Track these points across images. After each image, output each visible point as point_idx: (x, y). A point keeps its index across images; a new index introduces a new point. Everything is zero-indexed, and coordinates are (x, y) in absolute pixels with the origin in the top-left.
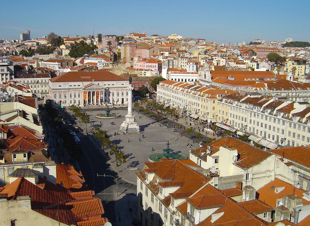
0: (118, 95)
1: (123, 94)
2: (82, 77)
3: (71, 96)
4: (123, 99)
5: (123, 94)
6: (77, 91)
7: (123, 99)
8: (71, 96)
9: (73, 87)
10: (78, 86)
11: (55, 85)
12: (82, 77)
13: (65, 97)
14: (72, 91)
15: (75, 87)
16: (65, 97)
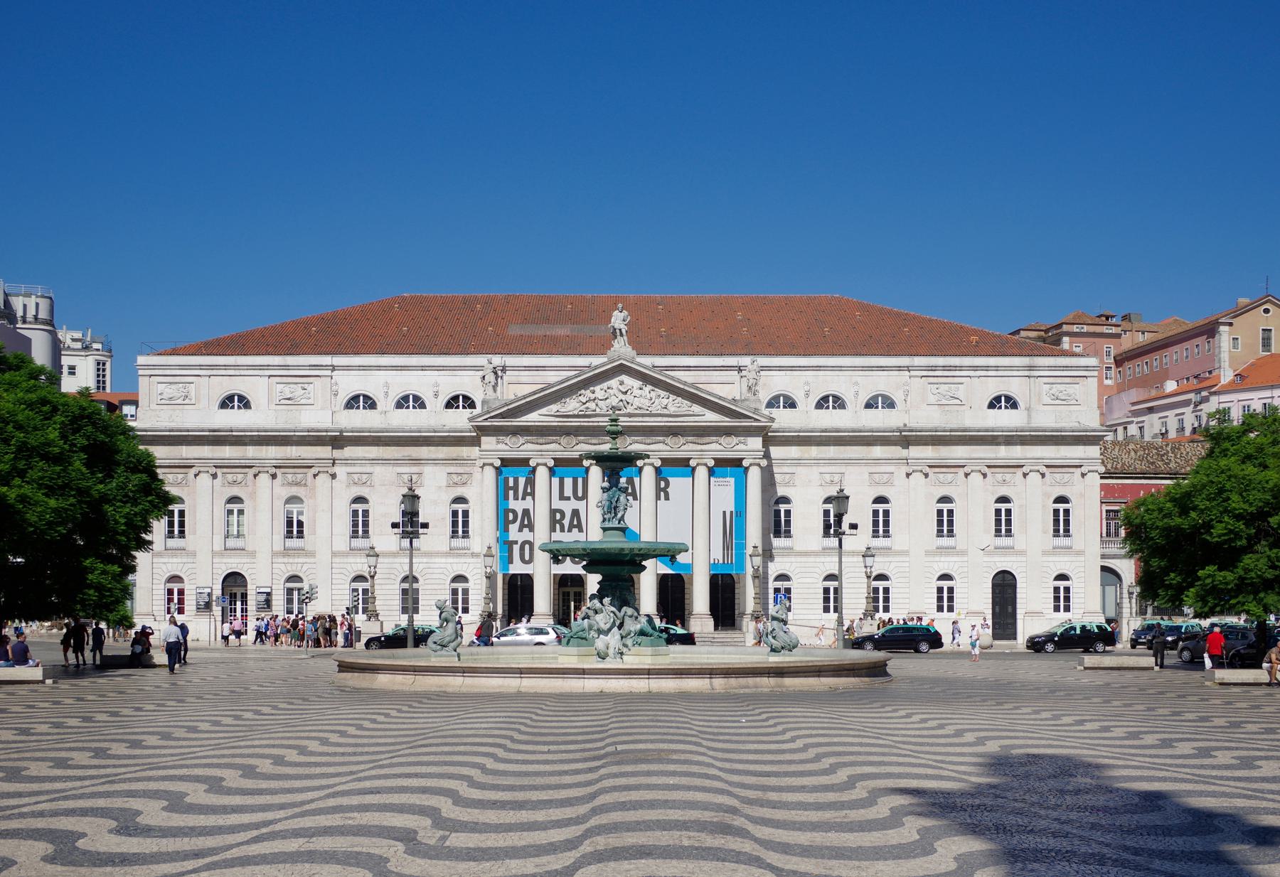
0: (945, 523)
1: (1003, 523)
2: (515, 330)
3: (360, 525)
4: (1004, 588)
5: (1003, 523)
6: (428, 470)
7: (1004, 588)
8: (360, 525)
9: (387, 418)
10: (452, 403)
11: (170, 391)
12: (515, 330)
13: (294, 528)
14: (378, 470)
15: (410, 420)
16: (294, 528)
